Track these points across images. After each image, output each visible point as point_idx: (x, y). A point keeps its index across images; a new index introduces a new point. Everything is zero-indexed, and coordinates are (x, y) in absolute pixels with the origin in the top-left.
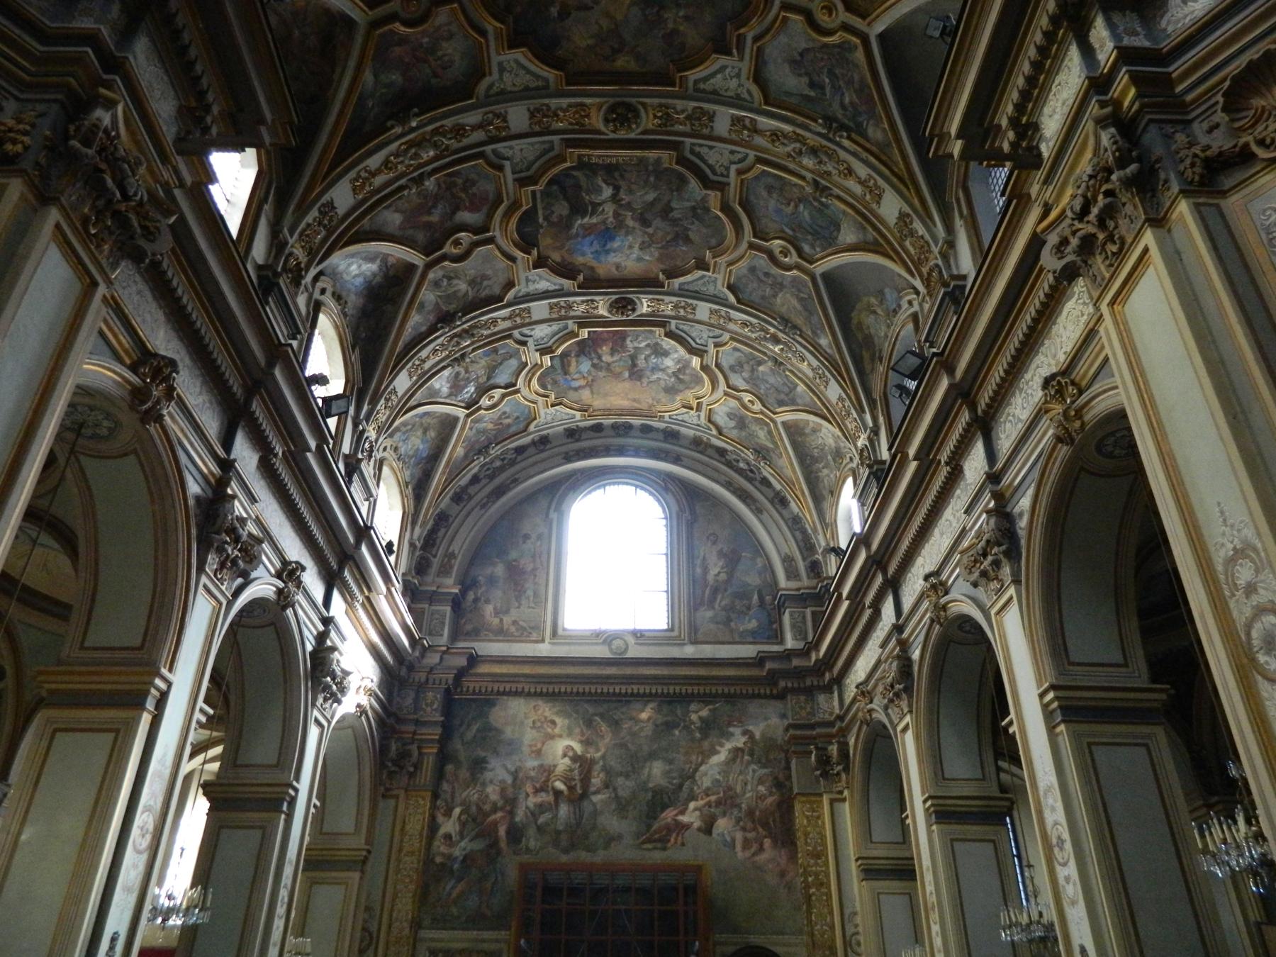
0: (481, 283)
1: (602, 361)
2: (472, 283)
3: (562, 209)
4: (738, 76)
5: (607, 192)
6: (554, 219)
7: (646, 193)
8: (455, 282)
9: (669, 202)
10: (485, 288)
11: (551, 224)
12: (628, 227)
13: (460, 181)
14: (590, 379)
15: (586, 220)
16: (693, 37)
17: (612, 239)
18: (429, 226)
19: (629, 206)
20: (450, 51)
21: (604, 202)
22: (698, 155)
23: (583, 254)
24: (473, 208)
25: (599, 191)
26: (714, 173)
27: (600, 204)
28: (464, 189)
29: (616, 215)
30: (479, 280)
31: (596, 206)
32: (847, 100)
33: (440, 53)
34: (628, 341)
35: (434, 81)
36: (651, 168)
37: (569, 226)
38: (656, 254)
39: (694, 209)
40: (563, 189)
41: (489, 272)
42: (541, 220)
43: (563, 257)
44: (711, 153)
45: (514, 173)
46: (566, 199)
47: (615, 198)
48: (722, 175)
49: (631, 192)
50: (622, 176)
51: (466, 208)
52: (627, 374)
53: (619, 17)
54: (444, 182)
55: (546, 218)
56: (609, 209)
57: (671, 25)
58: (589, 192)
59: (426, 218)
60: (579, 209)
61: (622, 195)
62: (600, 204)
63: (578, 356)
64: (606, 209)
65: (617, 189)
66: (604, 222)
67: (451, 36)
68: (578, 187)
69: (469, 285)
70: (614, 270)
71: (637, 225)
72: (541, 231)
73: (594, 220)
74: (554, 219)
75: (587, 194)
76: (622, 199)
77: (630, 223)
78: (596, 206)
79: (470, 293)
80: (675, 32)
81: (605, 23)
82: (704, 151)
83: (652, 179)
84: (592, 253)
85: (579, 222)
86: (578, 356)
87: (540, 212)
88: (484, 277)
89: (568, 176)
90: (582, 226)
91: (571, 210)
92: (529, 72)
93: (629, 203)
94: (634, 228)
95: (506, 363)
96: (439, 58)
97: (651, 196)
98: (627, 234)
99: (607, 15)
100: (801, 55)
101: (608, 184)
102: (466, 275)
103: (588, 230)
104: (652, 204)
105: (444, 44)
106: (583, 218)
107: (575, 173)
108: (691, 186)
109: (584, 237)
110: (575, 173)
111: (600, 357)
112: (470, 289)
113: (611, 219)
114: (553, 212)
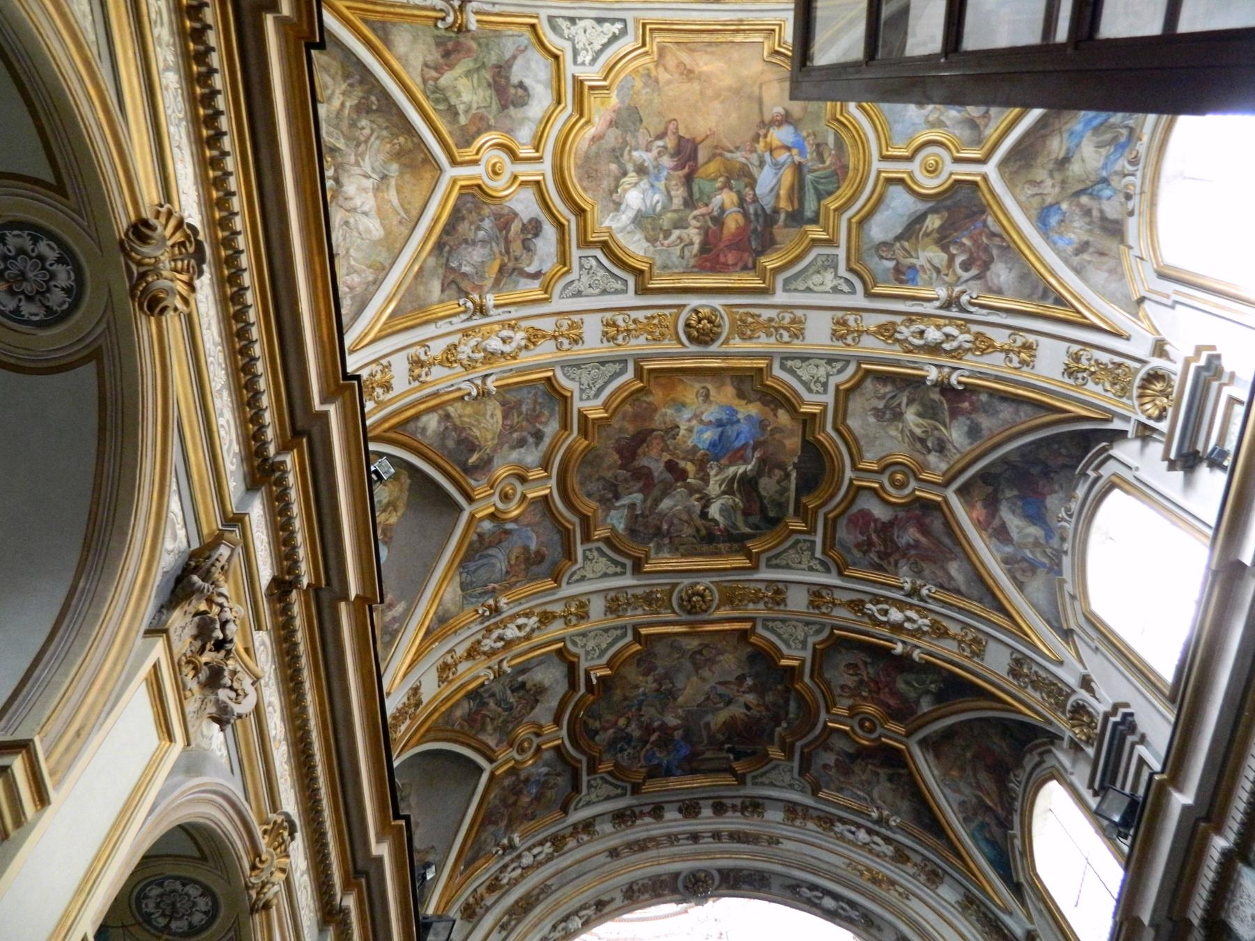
0: (886, 407)
1: (739, 193)
2: (898, 416)
3: (768, 486)
4: (587, 653)
5: (714, 511)
6: (778, 473)
7: (671, 509)
8: (918, 431)
9: (644, 501)
10: (883, 397)
11: (782, 466)
12: (692, 461)
13: (873, 556)
14: (761, 146)
15: (741, 470)
16: (631, 673)
17: (713, 445)
18: (925, 531)
19: (692, 490)
20: (846, 676)
21: (718, 497)
22: (616, 563)
23: (749, 418)
24: (866, 515)
25: (723, 510)
26: (599, 549)
27: (724, 493)
28: (870, 544)
29: (705, 478)
30: (887, 416)
31: (729, 491)
32: (492, 704)
33: (855, 678)
34: (697, 240)
35: (869, 660)
36: (666, 541)
37: (763, 461)
38: (657, 417)
39: (617, 497)
40: (763, 510)
41: (872, 420)
42: (794, 475)
43: (775, 415)
44: (604, 570)
45: (813, 543)
46: (761, 498)
47: (707, 501)
48: (590, 550)
49: (689, 510)
50: (698, 531)
51: (876, 521)
52: (702, 155)
53: (695, 679)
54: (889, 563)
55: (788, 475)
56: (713, 488)
57: (650, 679)
58: (734, 508)
59: (923, 540)
60: (747, 485)
61: (698, 506)
62: (724, 493)
63: (776, 211)
64: (717, 488)
65: (704, 515)
66: (721, 470)
67: (843, 687)
68: (746, 513)
69: (901, 414)
70: (713, 392)
71: (682, 464)
72: (796, 460)
73: (732, 470)
74: (778, 473)
75: (736, 505)
76: (699, 500)
77: (690, 467)
78: (729, 491)
79: (905, 400)
80: (646, 674)
81: (706, 673)
82: (612, 570)
83: (665, 527)
84: (738, 421)
85: (749, 467)
86: (776, 211)
87: (793, 486)
88: (879, 414)
89: (756, 527)
90: (746, 462)
91: (757, 483)
92: (779, 636)
93: (691, 494)
94: (683, 459)
95: (890, 237)
96: (857, 675)
97: (666, 504)
98: (695, 449)
99: (703, 680)
100: (537, 701)
101: (714, 520)
102: (902, 432)
103: (738, 456)
104: (665, 493)
105: (850, 684)
106: (745, 472)
107: (748, 530)
108: (622, 526)
109: (745, 446)
110: (748, 530)
111: (742, 202)
112: (903, 405)
113: (712, 473)
114: (778, 482)
